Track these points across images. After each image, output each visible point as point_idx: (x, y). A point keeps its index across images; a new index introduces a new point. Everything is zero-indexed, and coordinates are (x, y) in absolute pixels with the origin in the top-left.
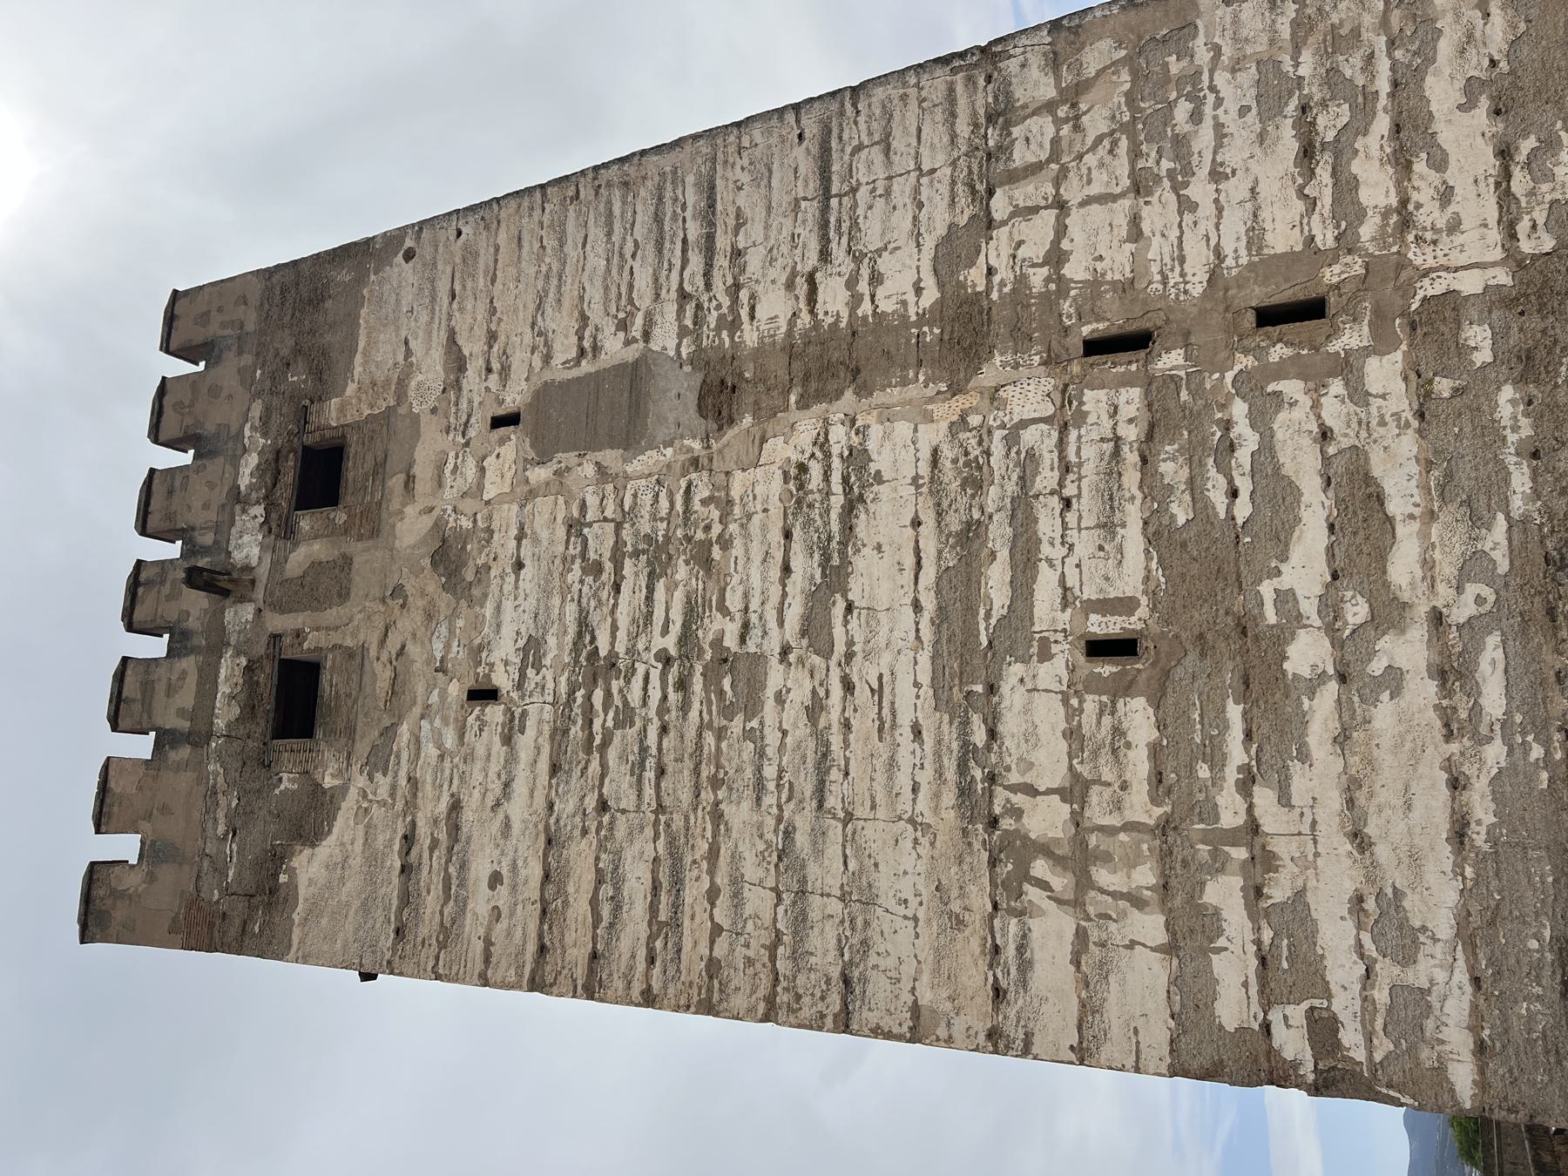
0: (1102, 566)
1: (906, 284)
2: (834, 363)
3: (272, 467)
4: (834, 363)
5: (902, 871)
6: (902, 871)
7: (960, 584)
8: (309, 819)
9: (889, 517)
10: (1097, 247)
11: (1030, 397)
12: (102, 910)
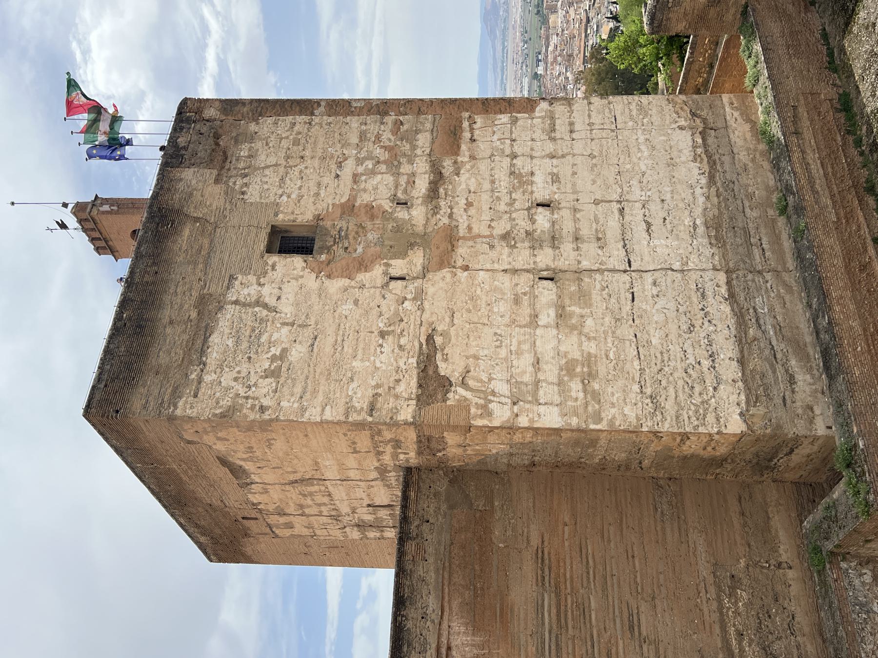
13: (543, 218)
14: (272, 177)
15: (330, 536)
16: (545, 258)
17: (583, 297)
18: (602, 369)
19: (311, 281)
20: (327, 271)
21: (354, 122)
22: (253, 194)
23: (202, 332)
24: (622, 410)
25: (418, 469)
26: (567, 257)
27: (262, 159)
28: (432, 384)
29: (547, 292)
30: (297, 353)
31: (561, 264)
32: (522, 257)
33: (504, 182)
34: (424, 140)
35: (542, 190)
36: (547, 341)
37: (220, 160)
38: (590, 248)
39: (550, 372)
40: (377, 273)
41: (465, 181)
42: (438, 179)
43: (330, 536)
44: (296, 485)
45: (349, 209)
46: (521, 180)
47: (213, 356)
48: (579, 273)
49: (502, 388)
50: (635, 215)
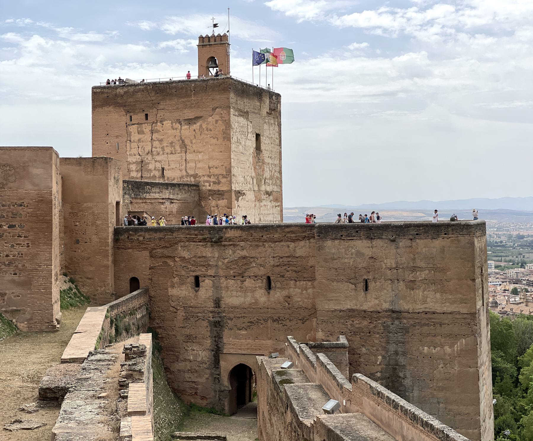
15: (131, 148)
21: (278, 162)
25: (199, 190)
40: (254, 174)
43: (131, 148)
44: (181, 142)
45: (264, 163)
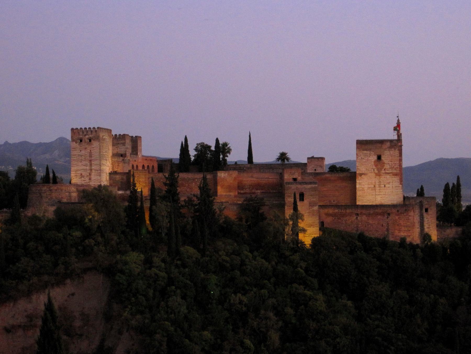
0: (84, 174)
1: (93, 168)
2: (91, 165)
3: (90, 137)
4: (91, 165)
5: (75, 168)
6: (75, 168)
7: (83, 170)
8: (76, 143)
9: (85, 167)
10: (93, 174)
11: (89, 172)
12: (72, 129)
13: (383, 186)
14: (389, 153)
16: (377, 186)
17: (372, 190)
18: (363, 192)
19: (373, 160)
20: (375, 162)
21: (398, 162)
22: (385, 152)
23: (366, 150)
24: (358, 193)
26: (377, 188)
27: (391, 152)
28: (361, 175)
29: (373, 186)
30: (364, 160)
31: (376, 188)
32: (377, 183)
33: (388, 181)
34: (395, 171)
35: (387, 186)
36: (366, 186)
37: (391, 147)
38: (379, 191)
39: (363, 186)
40: (374, 167)
41: (388, 176)
42: (388, 173)
45: (384, 163)
46: (389, 183)
47: (363, 152)
48: (375, 190)
49: (361, 182)
50: (384, 196)
